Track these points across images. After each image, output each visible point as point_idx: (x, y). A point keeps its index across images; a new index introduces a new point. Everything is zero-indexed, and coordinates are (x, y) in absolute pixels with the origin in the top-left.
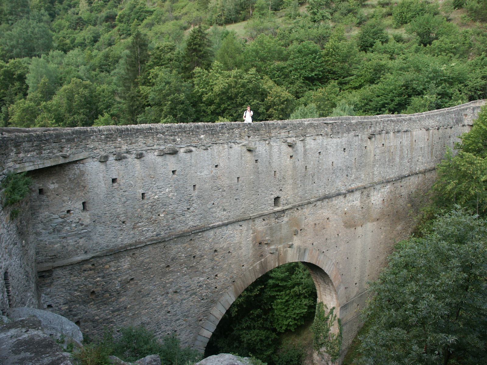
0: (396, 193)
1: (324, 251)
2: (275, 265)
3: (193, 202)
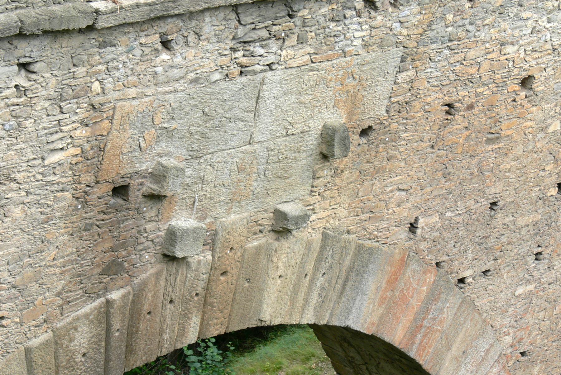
1: (467, 273)
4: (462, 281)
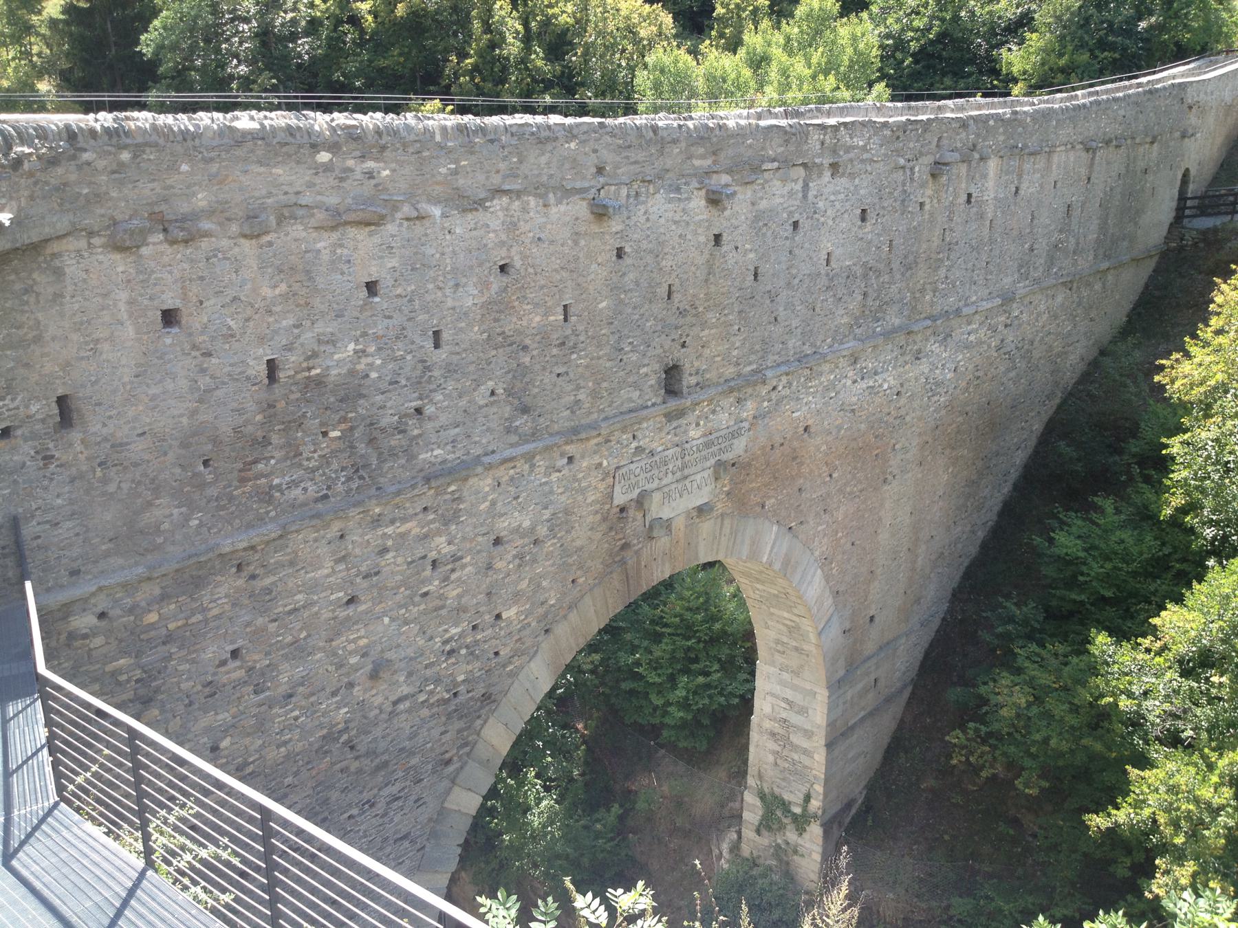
0: (989, 346)
2: (662, 572)
3: (433, 387)
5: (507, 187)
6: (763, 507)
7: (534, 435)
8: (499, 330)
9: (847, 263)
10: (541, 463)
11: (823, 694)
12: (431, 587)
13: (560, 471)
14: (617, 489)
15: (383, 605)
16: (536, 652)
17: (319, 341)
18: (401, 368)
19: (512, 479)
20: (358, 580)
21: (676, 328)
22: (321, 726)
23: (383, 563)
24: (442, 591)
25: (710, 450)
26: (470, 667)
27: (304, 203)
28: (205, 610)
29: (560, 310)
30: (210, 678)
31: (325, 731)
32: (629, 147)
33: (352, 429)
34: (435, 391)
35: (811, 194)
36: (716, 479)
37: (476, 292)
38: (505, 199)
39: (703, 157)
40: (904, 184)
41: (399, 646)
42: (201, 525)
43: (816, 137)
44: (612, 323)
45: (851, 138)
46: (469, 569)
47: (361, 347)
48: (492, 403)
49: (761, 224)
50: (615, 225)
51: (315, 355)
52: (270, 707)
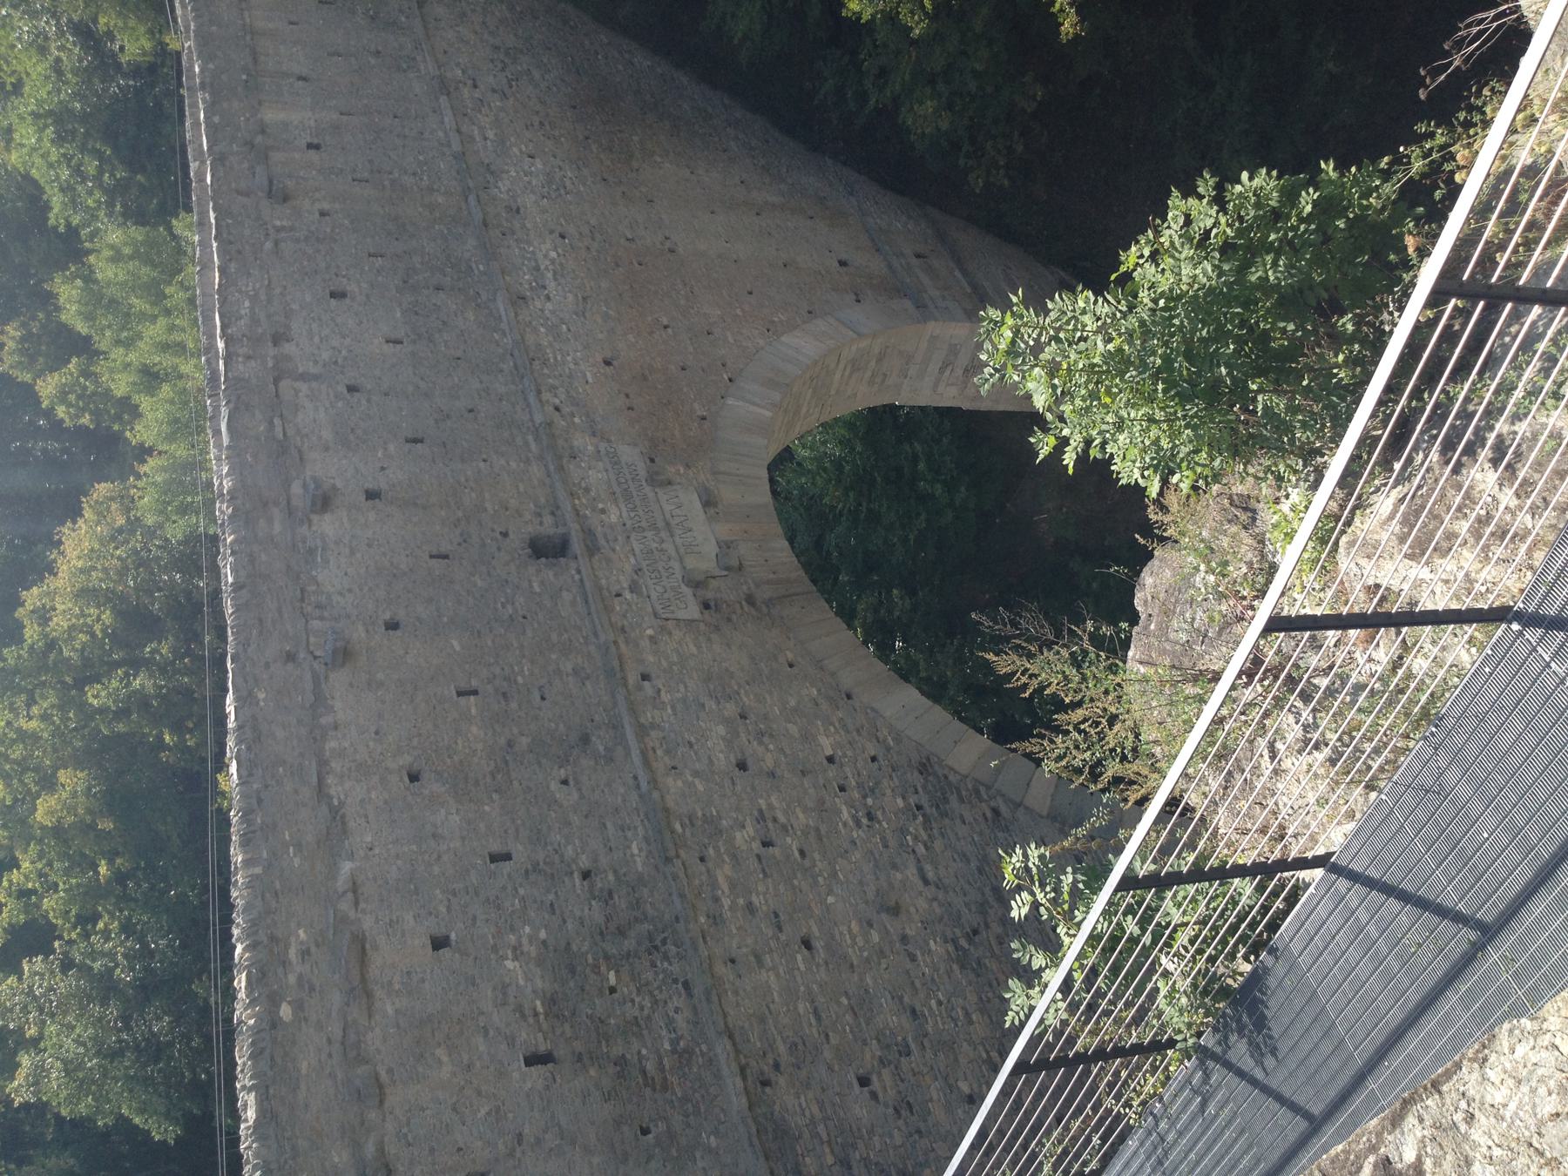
3: (557, 858)
4: (730, 380)
5: (315, 779)
6: (704, 418)
7: (616, 726)
8: (488, 779)
9: (399, 315)
10: (649, 716)
11: (933, 328)
12: (794, 848)
13: (659, 691)
14: (682, 615)
15: (813, 905)
16: (873, 709)
17: (504, 1004)
18: (535, 901)
19: (668, 752)
20: (783, 937)
21: (484, 545)
22: (949, 973)
23: (764, 908)
24: (799, 833)
25: (635, 494)
26: (888, 792)
27: (341, 1034)
28: (813, 1122)
29: (463, 700)
30: (891, 1110)
31: (955, 967)
32: (261, 620)
33: (607, 958)
34: (562, 856)
35: (313, 370)
36: (670, 483)
37: (443, 811)
38: (330, 780)
39: (270, 521)
40: (297, 241)
41: (861, 883)
42: (716, 1133)
43: (241, 367)
44: (479, 632)
45: (241, 318)
46: (773, 799)
47: (509, 952)
48: (577, 782)
49: (352, 437)
50: (358, 633)
51: (519, 1009)
52: (926, 1035)
